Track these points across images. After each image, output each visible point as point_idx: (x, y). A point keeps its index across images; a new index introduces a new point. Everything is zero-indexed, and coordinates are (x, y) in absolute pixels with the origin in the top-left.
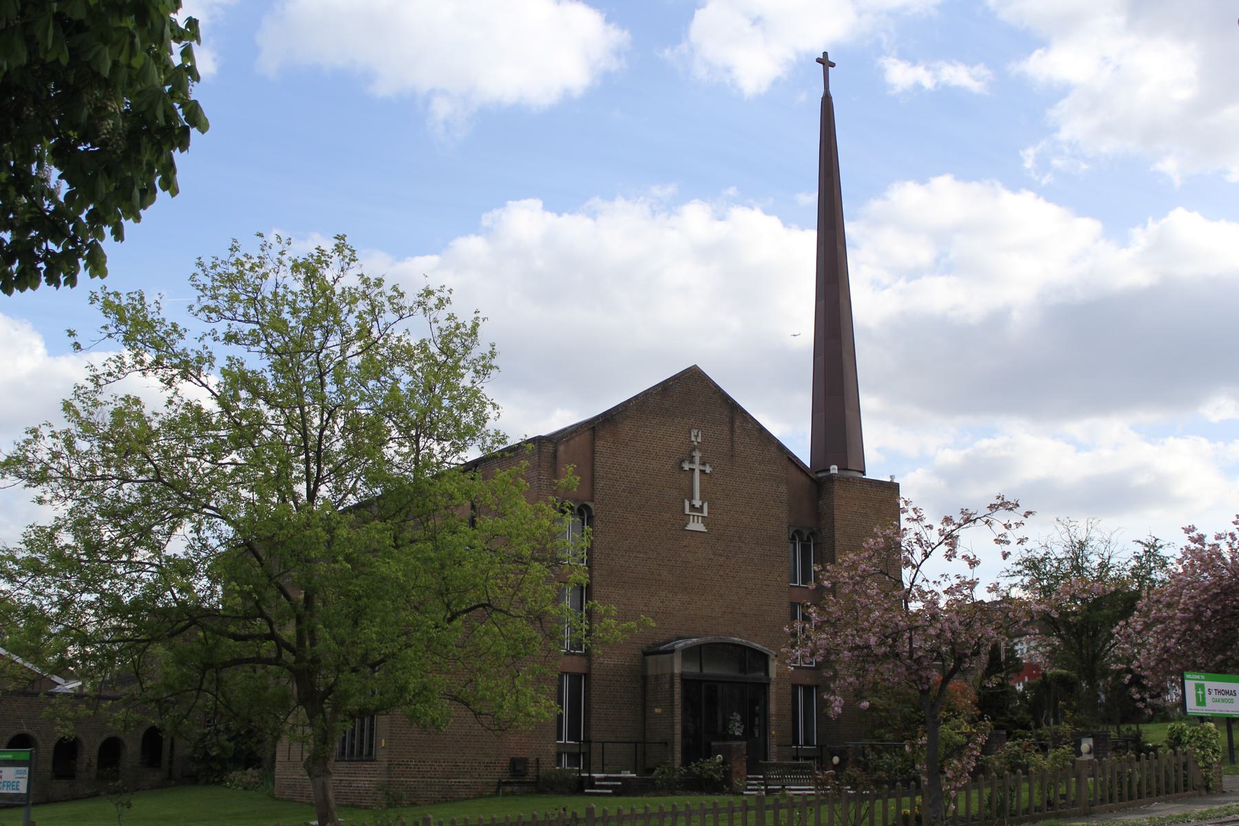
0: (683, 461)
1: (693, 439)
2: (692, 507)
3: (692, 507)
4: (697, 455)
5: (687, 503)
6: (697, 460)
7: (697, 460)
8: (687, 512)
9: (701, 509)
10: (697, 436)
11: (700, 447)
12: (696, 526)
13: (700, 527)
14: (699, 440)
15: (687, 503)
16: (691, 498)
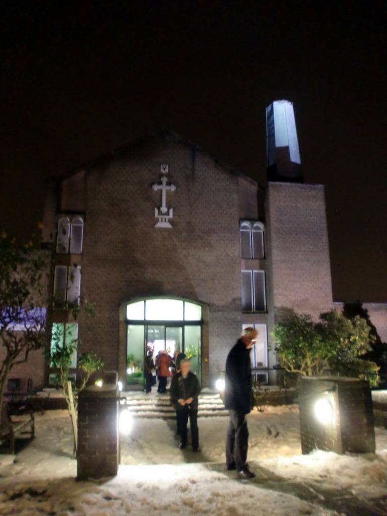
0: (153, 184)
1: (162, 170)
2: (160, 213)
3: (160, 213)
4: (164, 180)
5: (156, 210)
6: (164, 183)
7: (164, 183)
8: (156, 215)
9: (167, 214)
10: (164, 169)
11: (168, 175)
12: (164, 225)
13: (167, 225)
14: (167, 170)
15: (156, 210)
16: (161, 205)
